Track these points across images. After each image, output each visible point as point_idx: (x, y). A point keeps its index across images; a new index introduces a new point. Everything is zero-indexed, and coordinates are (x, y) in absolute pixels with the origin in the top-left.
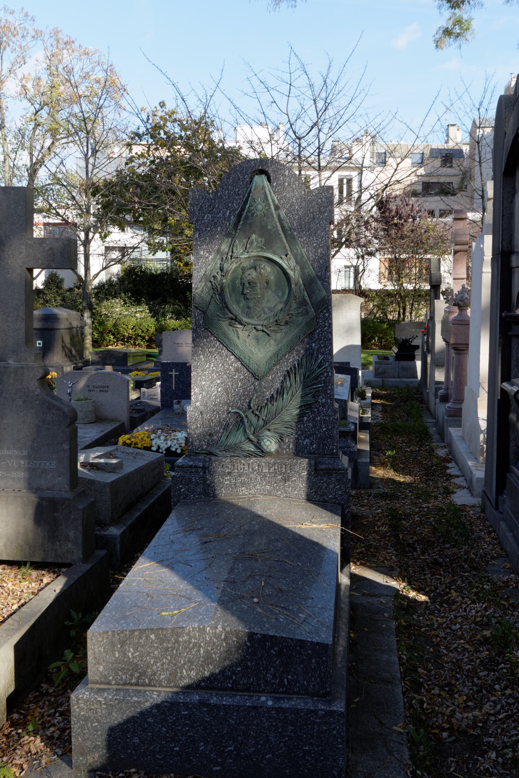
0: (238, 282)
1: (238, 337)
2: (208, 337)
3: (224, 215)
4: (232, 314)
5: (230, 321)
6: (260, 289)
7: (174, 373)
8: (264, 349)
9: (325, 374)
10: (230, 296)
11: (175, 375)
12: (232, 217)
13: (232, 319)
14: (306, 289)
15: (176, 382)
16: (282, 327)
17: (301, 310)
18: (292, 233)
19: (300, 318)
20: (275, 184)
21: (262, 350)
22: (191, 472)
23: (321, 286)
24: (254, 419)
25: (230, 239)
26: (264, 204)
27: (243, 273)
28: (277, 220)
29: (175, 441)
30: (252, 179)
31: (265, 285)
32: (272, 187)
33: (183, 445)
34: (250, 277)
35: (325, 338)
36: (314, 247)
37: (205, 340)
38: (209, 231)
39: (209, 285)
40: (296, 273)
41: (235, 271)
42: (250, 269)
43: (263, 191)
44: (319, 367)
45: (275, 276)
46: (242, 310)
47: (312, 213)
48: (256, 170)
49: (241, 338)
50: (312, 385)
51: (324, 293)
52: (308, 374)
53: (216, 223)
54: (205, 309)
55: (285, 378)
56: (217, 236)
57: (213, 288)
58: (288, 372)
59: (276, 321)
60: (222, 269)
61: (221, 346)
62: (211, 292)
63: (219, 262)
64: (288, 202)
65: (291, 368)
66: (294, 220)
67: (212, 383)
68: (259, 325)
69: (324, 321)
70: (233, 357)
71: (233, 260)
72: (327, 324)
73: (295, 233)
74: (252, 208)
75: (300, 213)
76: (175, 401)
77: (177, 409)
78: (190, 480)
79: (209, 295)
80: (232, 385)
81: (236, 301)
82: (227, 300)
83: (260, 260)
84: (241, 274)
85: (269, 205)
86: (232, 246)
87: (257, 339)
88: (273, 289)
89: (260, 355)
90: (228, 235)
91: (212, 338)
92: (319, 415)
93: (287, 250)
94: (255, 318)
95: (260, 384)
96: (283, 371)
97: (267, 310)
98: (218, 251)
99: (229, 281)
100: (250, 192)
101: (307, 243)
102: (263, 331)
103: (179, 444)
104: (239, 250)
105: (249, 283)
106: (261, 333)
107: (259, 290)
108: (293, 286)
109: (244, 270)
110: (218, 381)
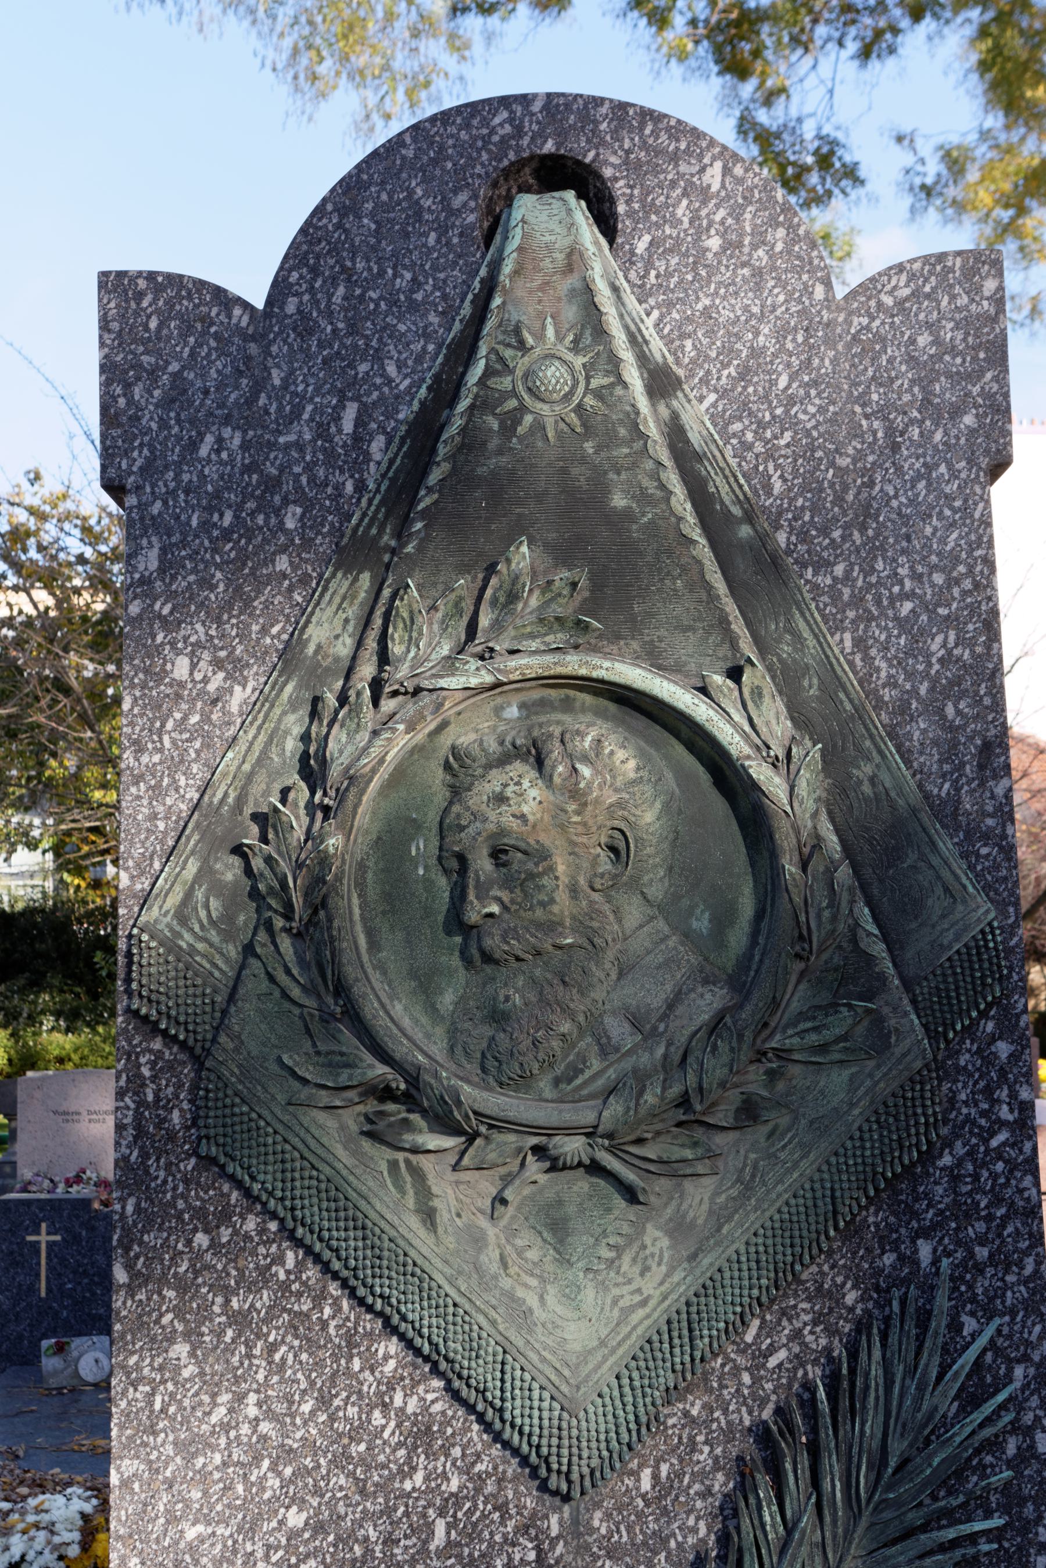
0: (422, 847)
1: (429, 1216)
2: (225, 1216)
3: (322, 432)
4: (384, 1057)
5: (372, 1106)
6: (574, 891)
7: (43, 1238)
8: (603, 1287)
9: (1011, 1449)
10: (374, 945)
11: (50, 1245)
12: (377, 446)
13: (386, 1094)
14: (864, 887)
15: (50, 1268)
16: (720, 1140)
17: (840, 1023)
18: (763, 539)
19: (838, 1079)
20: (641, 246)
21: (589, 1294)
23: (959, 866)
25: (365, 579)
26: (579, 361)
27: (456, 792)
28: (664, 455)
29: (42, 1536)
30: (494, 226)
31: (605, 863)
32: (628, 261)
33: (74, 1551)
34: (505, 817)
35: (997, 1200)
36: (904, 624)
37: (201, 1239)
38: (226, 534)
39: (230, 870)
40: (803, 788)
41: (400, 776)
42: (503, 761)
43: (572, 281)
44: (970, 1399)
45: (666, 807)
46: (453, 1033)
47: (882, 413)
48: (519, 165)
49: (443, 1217)
50: (925, 1528)
51: (982, 910)
52: (897, 1448)
53: (271, 484)
54: (205, 1030)
55: (745, 1484)
56: (282, 563)
57: (254, 894)
58: (762, 1434)
59: (684, 1102)
60: (312, 768)
61: (312, 1273)
62: (246, 917)
63: (295, 724)
64: (728, 352)
65: (778, 1411)
66: (769, 455)
67: (249, 1529)
68: (569, 1130)
69: (988, 1092)
70: (393, 1346)
71: (388, 705)
72: (1005, 1113)
73: (782, 537)
74: (505, 383)
75: (806, 414)
76: (45, 1344)
77: (56, 1373)
79: (228, 936)
80: (390, 1541)
81: (413, 974)
82: (351, 972)
83: (567, 705)
84: (441, 796)
85: (614, 363)
86: (377, 624)
87: (556, 1227)
88: (656, 892)
89: (578, 1335)
90: (352, 553)
91: (251, 1224)
93: (733, 642)
94: (544, 1085)
95: (576, 1529)
96: (729, 1433)
97: (618, 1029)
98: (290, 655)
99: (361, 845)
100: (490, 286)
101: (857, 601)
102: (595, 1168)
103: (56, 1548)
104: (425, 646)
105: (497, 854)
106: (582, 1184)
107: (562, 897)
108: (790, 868)
109: (459, 768)
110: (295, 1519)
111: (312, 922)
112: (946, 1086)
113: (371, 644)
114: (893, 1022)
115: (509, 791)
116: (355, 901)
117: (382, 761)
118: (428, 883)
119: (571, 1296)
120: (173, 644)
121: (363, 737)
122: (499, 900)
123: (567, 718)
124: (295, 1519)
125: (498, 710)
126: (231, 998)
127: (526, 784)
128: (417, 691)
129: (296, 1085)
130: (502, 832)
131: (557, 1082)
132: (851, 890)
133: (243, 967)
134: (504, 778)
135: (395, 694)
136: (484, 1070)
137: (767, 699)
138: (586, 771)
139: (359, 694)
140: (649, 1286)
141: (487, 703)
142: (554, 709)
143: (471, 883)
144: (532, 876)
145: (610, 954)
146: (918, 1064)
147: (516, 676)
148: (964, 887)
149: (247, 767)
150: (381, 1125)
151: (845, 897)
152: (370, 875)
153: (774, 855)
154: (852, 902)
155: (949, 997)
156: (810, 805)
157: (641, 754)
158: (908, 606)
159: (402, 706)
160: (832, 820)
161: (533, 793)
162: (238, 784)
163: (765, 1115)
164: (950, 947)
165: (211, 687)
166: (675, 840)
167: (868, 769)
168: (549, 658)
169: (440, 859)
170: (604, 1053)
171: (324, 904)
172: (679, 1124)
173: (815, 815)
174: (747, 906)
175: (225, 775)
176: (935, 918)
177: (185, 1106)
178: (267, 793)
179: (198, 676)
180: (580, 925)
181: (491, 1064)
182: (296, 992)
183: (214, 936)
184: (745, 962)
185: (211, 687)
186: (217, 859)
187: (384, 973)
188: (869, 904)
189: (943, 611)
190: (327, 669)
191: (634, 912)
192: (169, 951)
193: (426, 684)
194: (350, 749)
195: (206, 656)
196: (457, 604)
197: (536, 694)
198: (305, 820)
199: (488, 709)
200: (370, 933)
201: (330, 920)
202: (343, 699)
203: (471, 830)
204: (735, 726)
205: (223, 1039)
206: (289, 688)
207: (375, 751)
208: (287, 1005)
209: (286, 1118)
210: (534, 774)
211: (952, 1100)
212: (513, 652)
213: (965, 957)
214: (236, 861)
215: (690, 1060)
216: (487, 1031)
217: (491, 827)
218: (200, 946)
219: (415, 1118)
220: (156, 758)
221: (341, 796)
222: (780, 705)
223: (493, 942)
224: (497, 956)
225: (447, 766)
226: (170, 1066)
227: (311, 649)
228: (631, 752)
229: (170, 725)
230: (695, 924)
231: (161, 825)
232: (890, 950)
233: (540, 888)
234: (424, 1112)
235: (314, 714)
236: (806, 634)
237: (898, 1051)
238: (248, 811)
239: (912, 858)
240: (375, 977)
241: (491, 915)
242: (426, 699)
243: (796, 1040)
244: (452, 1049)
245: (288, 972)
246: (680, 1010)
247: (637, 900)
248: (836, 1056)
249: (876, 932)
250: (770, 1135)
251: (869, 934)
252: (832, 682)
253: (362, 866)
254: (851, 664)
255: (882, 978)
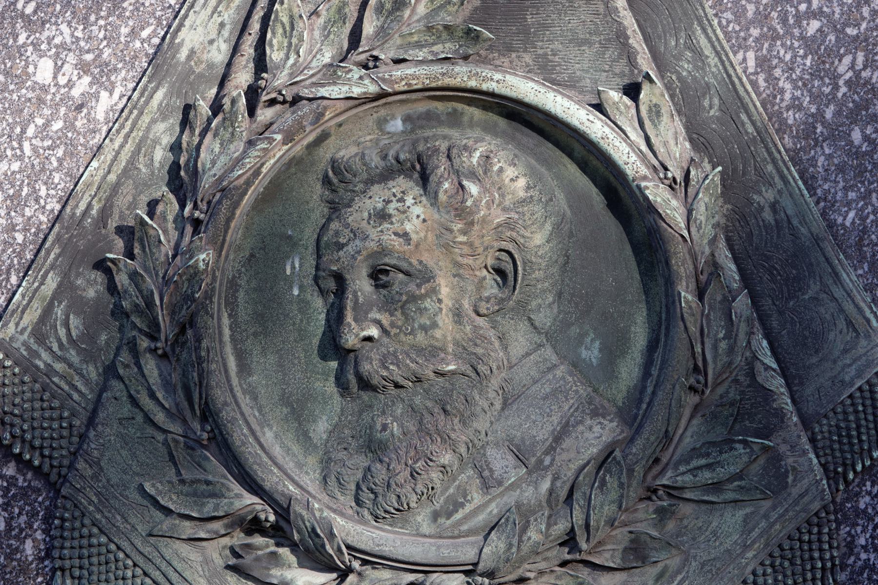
0: (298, 265)
4: (254, 486)
5: (238, 538)
6: (458, 315)
10: (244, 368)
13: (254, 526)
14: (763, 319)
17: (736, 460)
19: (731, 520)
31: (491, 288)
39: (92, 287)
40: (701, 212)
41: (277, 189)
42: (386, 176)
45: (557, 227)
46: (326, 462)
57: (118, 313)
59: (570, 541)
63: (164, 133)
71: (264, 114)
79: (89, 356)
81: (285, 400)
82: (219, 395)
83: (454, 120)
84: (318, 212)
88: (544, 318)
93: (631, 58)
94: (422, 518)
97: (500, 461)
99: (233, 263)
105: (378, 275)
107: (445, 321)
108: (686, 295)
109: (340, 184)
111: (179, 341)
112: (844, 530)
113: (248, 49)
114: (790, 461)
115: (392, 208)
116: (226, 321)
117: (257, 173)
118: (303, 304)
120: (36, 45)
121: (237, 147)
122: (378, 323)
123: (454, 133)
125: (381, 123)
126: (91, 422)
127: (409, 201)
128: (296, 100)
129: (158, 515)
130: (383, 251)
131: (436, 516)
132: (749, 321)
133: (104, 389)
134: (386, 194)
135: (272, 102)
136: (358, 502)
137: (665, 119)
138: (473, 188)
139: (234, 102)
141: (371, 115)
142: (440, 123)
143: (349, 304)
144: (413, 298)
145: (495, 383)
146: (816, 506)
147: (401, 87)
148: (868, 321)
149: (112, 178)
150: (248, 559)
151: (743, 328)
152: (241, 295)
153: (669, 282)
154: (750, 334)
155: (849, 436)
156: (708, 231)
157: (531, 173)
158: (814, 26)
159: (279, 115)
160: (731, 248)
161: (417, 210)
162: (103, 195)
163: (654, 556)
164: (852, 384)
165: (76, 92)
166: (566, 264)
167: (770, 195)
168: (437, 69)
169: (316, 279)
170: (486, 486)
171: (191, 322)
172: (564, 564)
173: (713, 241)
174: (639, 336)
175: (88, 186)
176: (837, 353)
177: (39, 535)
178: (133, 205)
179: (62, 80)
180: (463, 351)
181: (367, 496)
182: (160, 417)
183: (73, 355)
184: (637, 395)
185: (76, 92)
186: (78, 275)
187: (255, 398)
188: (767, 336)
189: (851, 31)
190: (201, 76)
191: (521, 340)
192: (25, 371)
193: (306, 93)
194: (223, 159)
195: (71, 58)
196: (340, 10)
197: (422, 107)
198: (174, 235)
199: (371, 121)
200: (241, 356)
201: (199, 340)
202: (216, 107)
203: (350, 249)
204: (631, 144)
205: (81, 465)
206: (159, 95)
207: (250, 162)
208: (150, 431)
209: (147, 550)
210: (418, 190)
211: (851, 545)
212: (398, 61)
213: (867, 395)
214: (98, 276)
215: (577, 495)
216: (362, 461)
217: (372, 245)
218: (59, 366)
219: (285, 552)
220: (16, 166)
221: (212, 208)
222: (679, 125)
223: (371, 367)
224: (376, 380)
225: (326, 181)
226: (24, 493)
227: (183, 55)
228: (521, 169)
229: (31, 131)
230: (584, 354)
231: (19, 237)
232: (788, 385)
233: (421, 311)
234: (294, 547)
235: (185, 122)
236: (708, 51)
237: (795, 491)
238: (112, 224)
239: (814, 288)
240: (245, 401)
241: (369, 339)
242: (305, 108)
243: (688, 478)
244: (325, 479)
245: (152, 395)
246: (567, 443)
247: (524, 326)
248: (730, 496)
249: (775, 366)
250: (659, 577)
251: (767, 368)
252: (734, 102)
253: (233, 285)
254: (754, 84)
255: (780, 414)
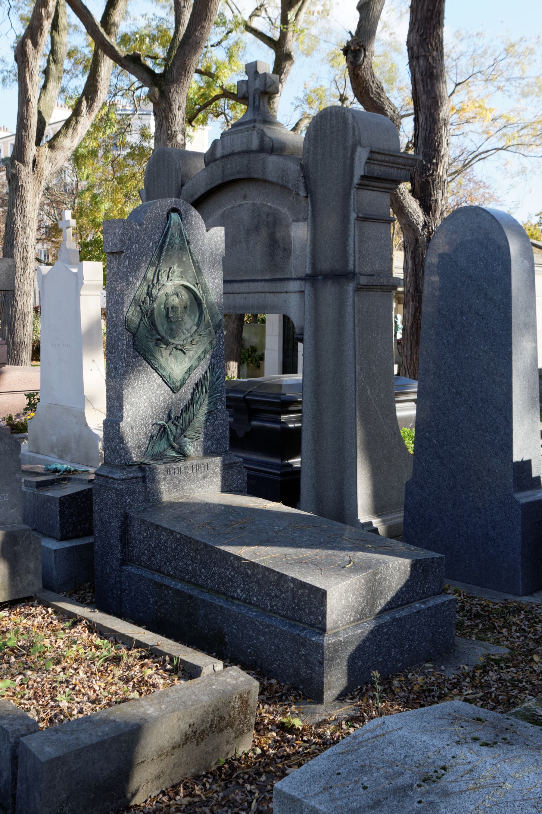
0: (163, 306)
1: (162, 356)
3: (148, 246)
19: (206, 338)
22: (133, 483)
24: (173, 428)
27: (167, 299)
34: (173, 303)
36: (213, 278)
39: (138, 309)
46: (166, 332)
53: (142, 253)
55: (194, 390)
57: (142, 312)
63: (146, 288)
67: (140, 399)
70: (156, 374)
78: (134, 491)
84: (165, 299)
90: (152, 264)
92: (217, 419)
95: (176, 396)
110: (145, 397)
119: (177, 367)
124: (145, 397)
140: (186, 365)
223: (172, 320)
